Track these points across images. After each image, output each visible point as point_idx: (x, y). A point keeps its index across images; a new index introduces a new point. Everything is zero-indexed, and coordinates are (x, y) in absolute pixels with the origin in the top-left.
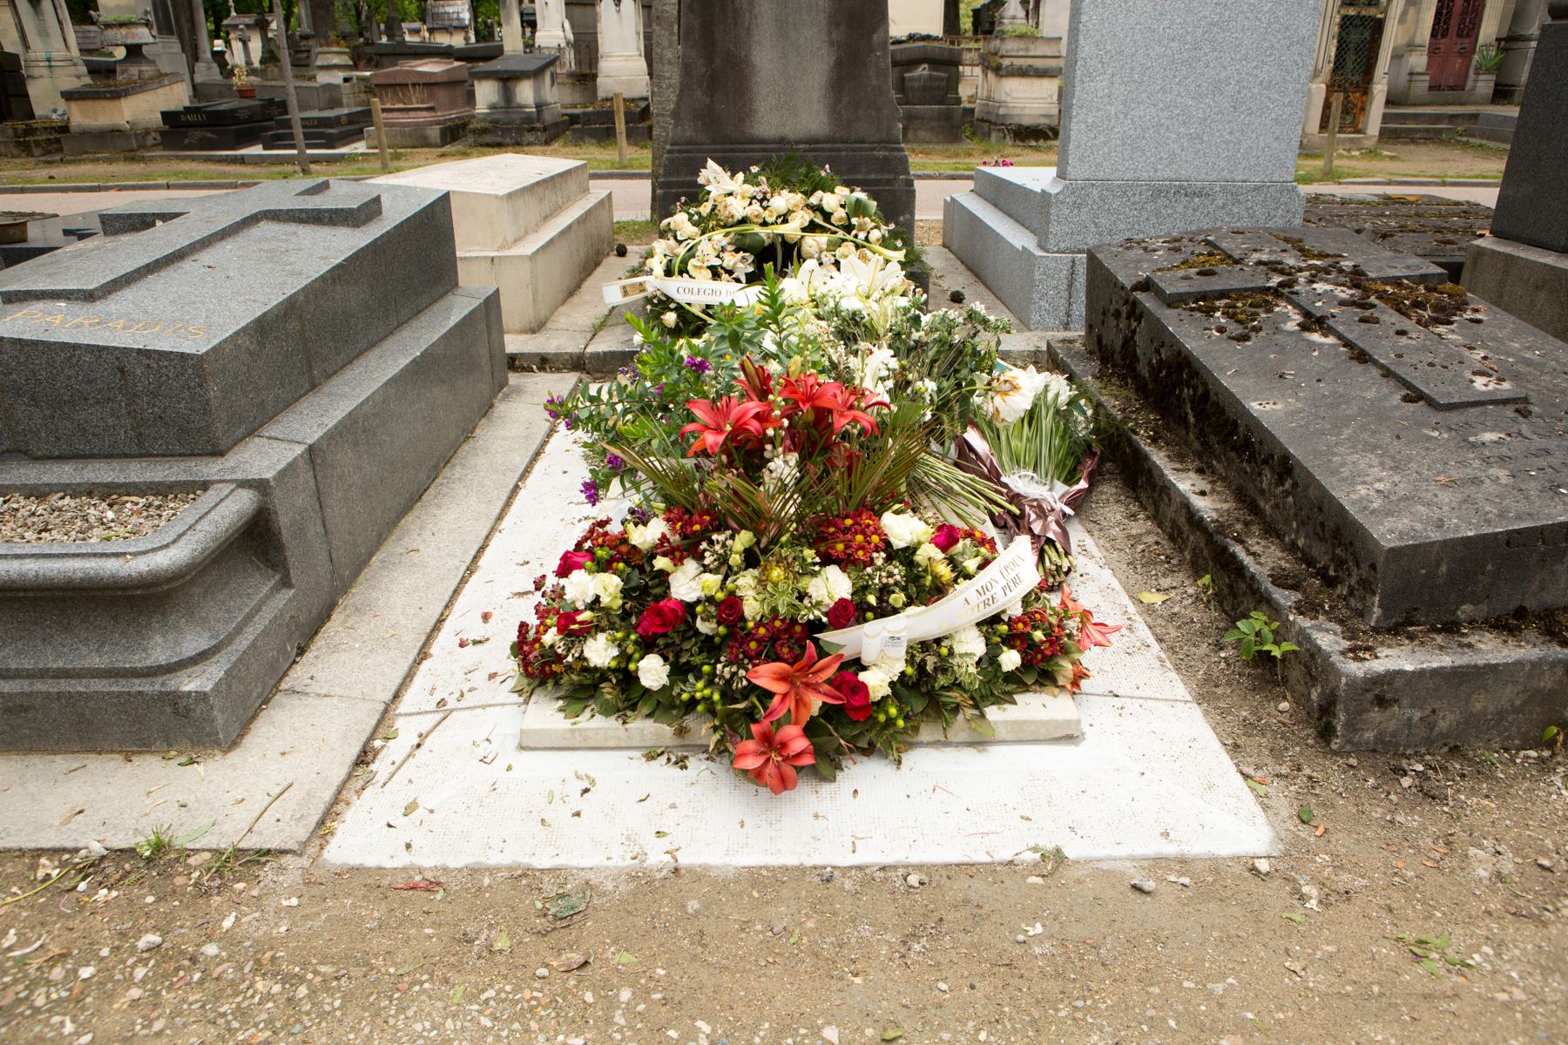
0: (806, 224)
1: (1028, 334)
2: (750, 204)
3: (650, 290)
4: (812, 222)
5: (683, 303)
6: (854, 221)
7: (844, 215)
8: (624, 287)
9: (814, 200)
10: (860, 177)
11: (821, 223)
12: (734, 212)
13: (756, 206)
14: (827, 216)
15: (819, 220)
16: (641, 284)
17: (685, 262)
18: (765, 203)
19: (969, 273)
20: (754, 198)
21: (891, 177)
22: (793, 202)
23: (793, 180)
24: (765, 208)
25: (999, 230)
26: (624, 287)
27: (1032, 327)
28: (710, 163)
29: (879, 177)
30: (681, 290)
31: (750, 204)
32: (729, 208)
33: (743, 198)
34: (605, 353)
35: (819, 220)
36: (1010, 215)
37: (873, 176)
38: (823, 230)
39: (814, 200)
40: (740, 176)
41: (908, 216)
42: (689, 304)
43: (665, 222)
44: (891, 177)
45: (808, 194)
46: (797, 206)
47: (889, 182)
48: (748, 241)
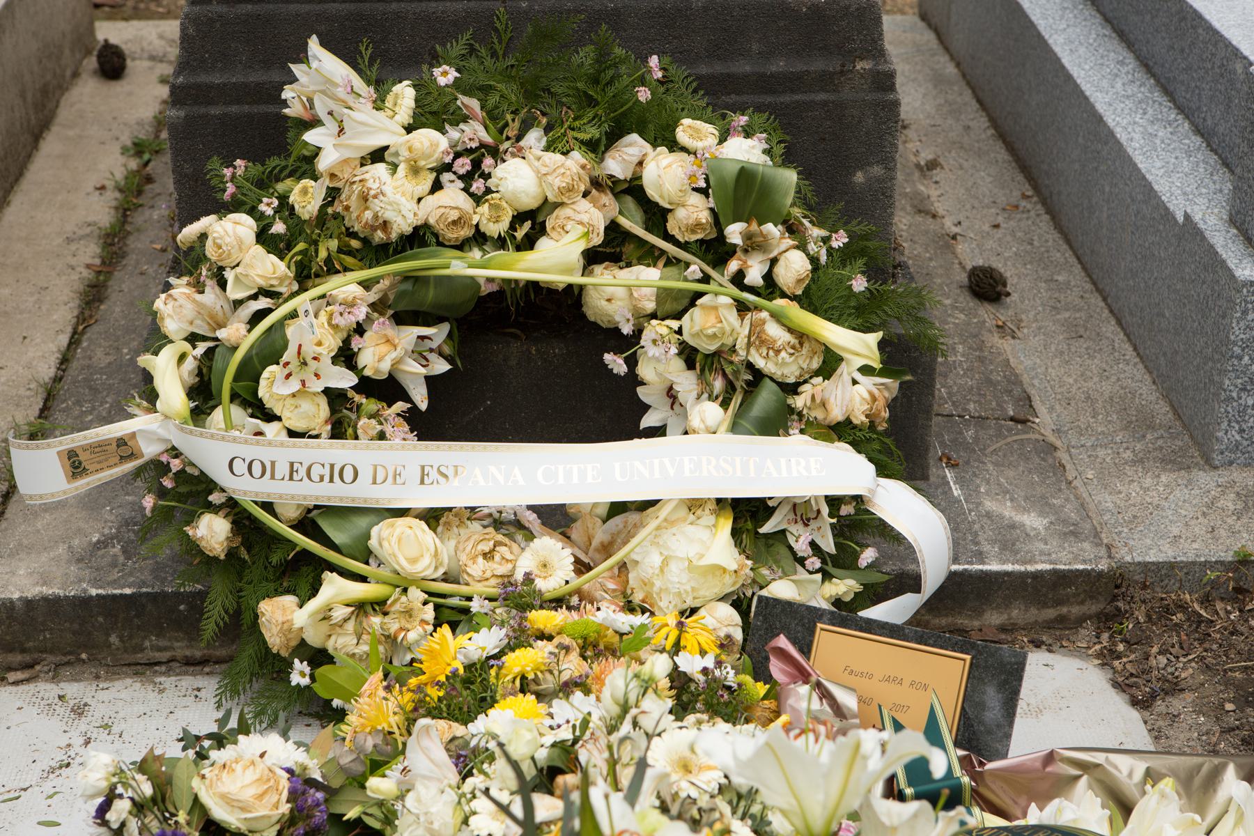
0: (598, 240)
1: (1205, 479)
2: (437, 186)
3: (149, 450)
4: (613, 228)
5: (246, 501)
6: (734, 233)
7: (705, 217)
8: (72, 455)
9: (616, 164)
10: (744, 67)
11: (639, 231)
12: (389, 215)
13: (453, 196)
14: (656, 216)
15: (633, 225)
16: (121, 442)
17: (250, 372)
18: (478, 186)
19: (1002, 154)
20: (448, 167)
21: (833, 65)
22: (558, 182)
23: (557, 88)
24: (478, 200)
25: (1101, 101)
26: (72, 455)
27: (1217, 459)
28: (293, 684)
29: (799, 67)
30: (240, 467)
31: (437, 186)
32: (376, 205)
33: (415, 171)
34: (29, 604)
35: (633, 225)
36: (1123, 36)
37: (779, 65)
38: (650, 255)
39: (616, 164)
40: (404, 95)
41: (877, 170)
42: (268, 507)
43: (190, 231)
44: (833, 65)
45: (596, 148)
46: (570, 189)
47: (826, 81)
48: (430, 296)
